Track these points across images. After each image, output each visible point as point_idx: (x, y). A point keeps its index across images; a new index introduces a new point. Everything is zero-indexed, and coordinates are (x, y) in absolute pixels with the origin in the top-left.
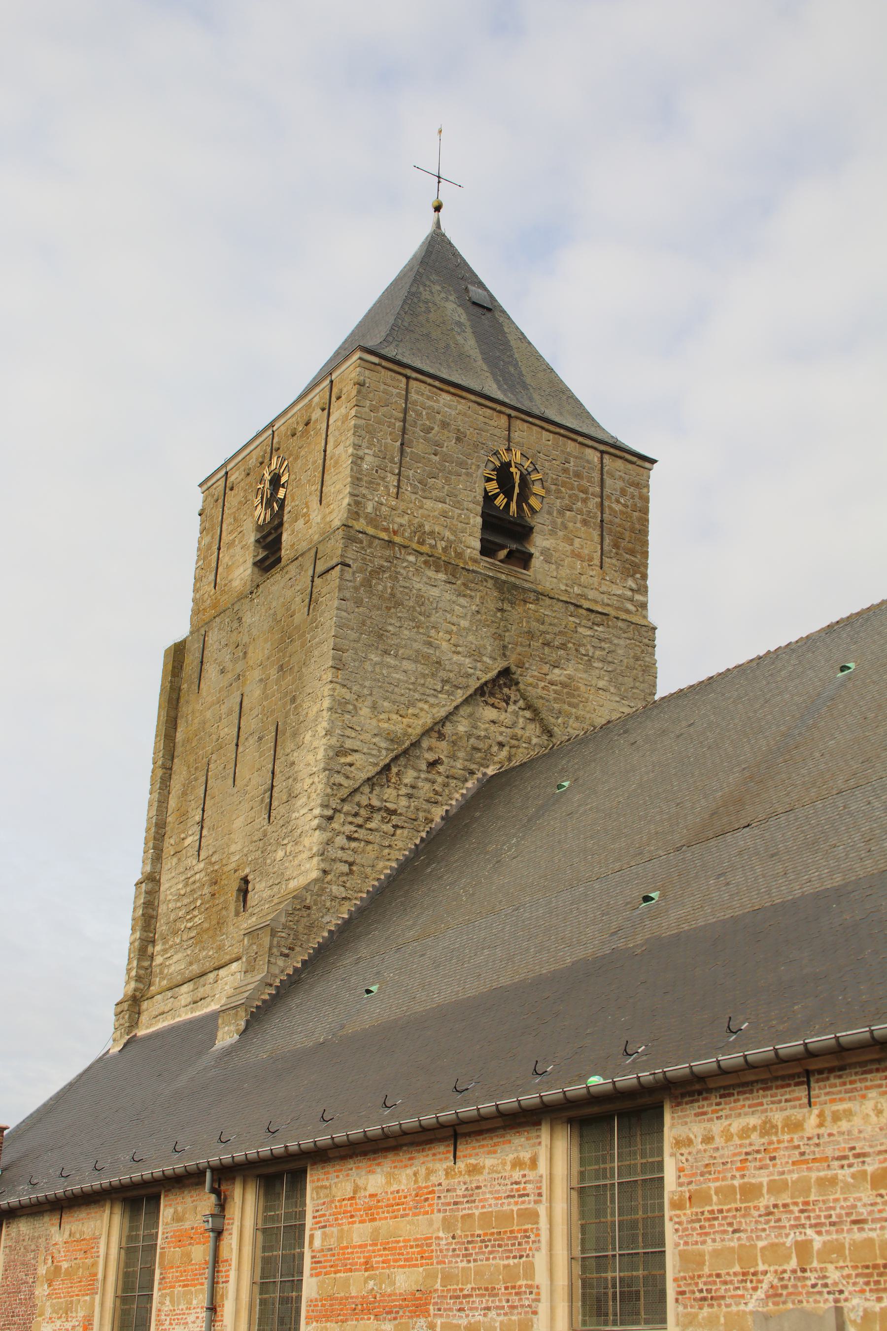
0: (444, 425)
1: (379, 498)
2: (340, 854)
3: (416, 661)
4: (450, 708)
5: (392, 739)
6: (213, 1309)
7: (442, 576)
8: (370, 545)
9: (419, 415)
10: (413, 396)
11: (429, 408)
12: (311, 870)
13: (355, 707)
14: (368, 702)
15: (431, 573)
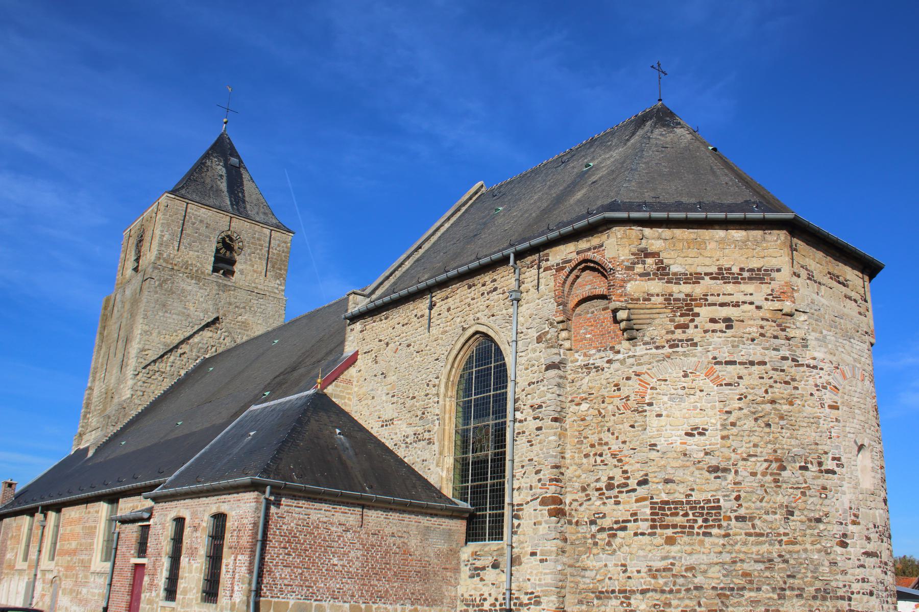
1: (171, 251)
4: (191, 333)
5: (165, 345)
6: (40, 551)
9: (190, 218)
10: (189, 210)
12: (127, 394)
14: (157, 331)
15: (189, 280)
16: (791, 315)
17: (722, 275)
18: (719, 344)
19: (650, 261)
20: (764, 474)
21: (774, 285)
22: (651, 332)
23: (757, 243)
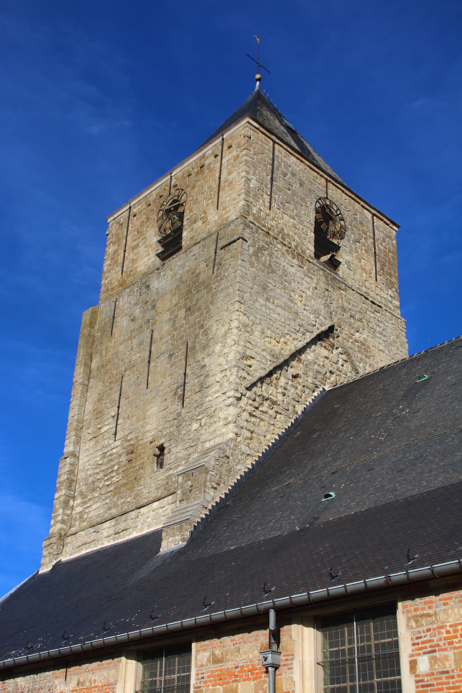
0: (293, 174)
1: (260, 206)
2: (245, 424)
3: (284, 309)
4: (303, 343)
7: (295, 261)
8: (257, 232)
11: (285, 162)
12: (229, 433)
13: (252, 330)
14: (259, 328)
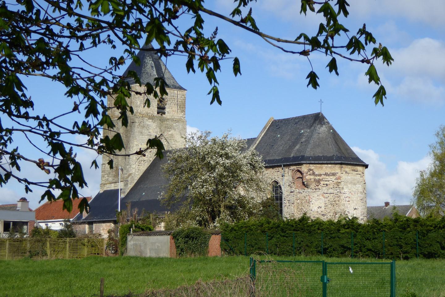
7: (151, 120)
16: (340, 183)
17: (326, 174)
18: (325, 189)
19: (311, 171)
20: (332, 216)
21: (337, 176)
22: (311, 186)
23: (334, 167)
